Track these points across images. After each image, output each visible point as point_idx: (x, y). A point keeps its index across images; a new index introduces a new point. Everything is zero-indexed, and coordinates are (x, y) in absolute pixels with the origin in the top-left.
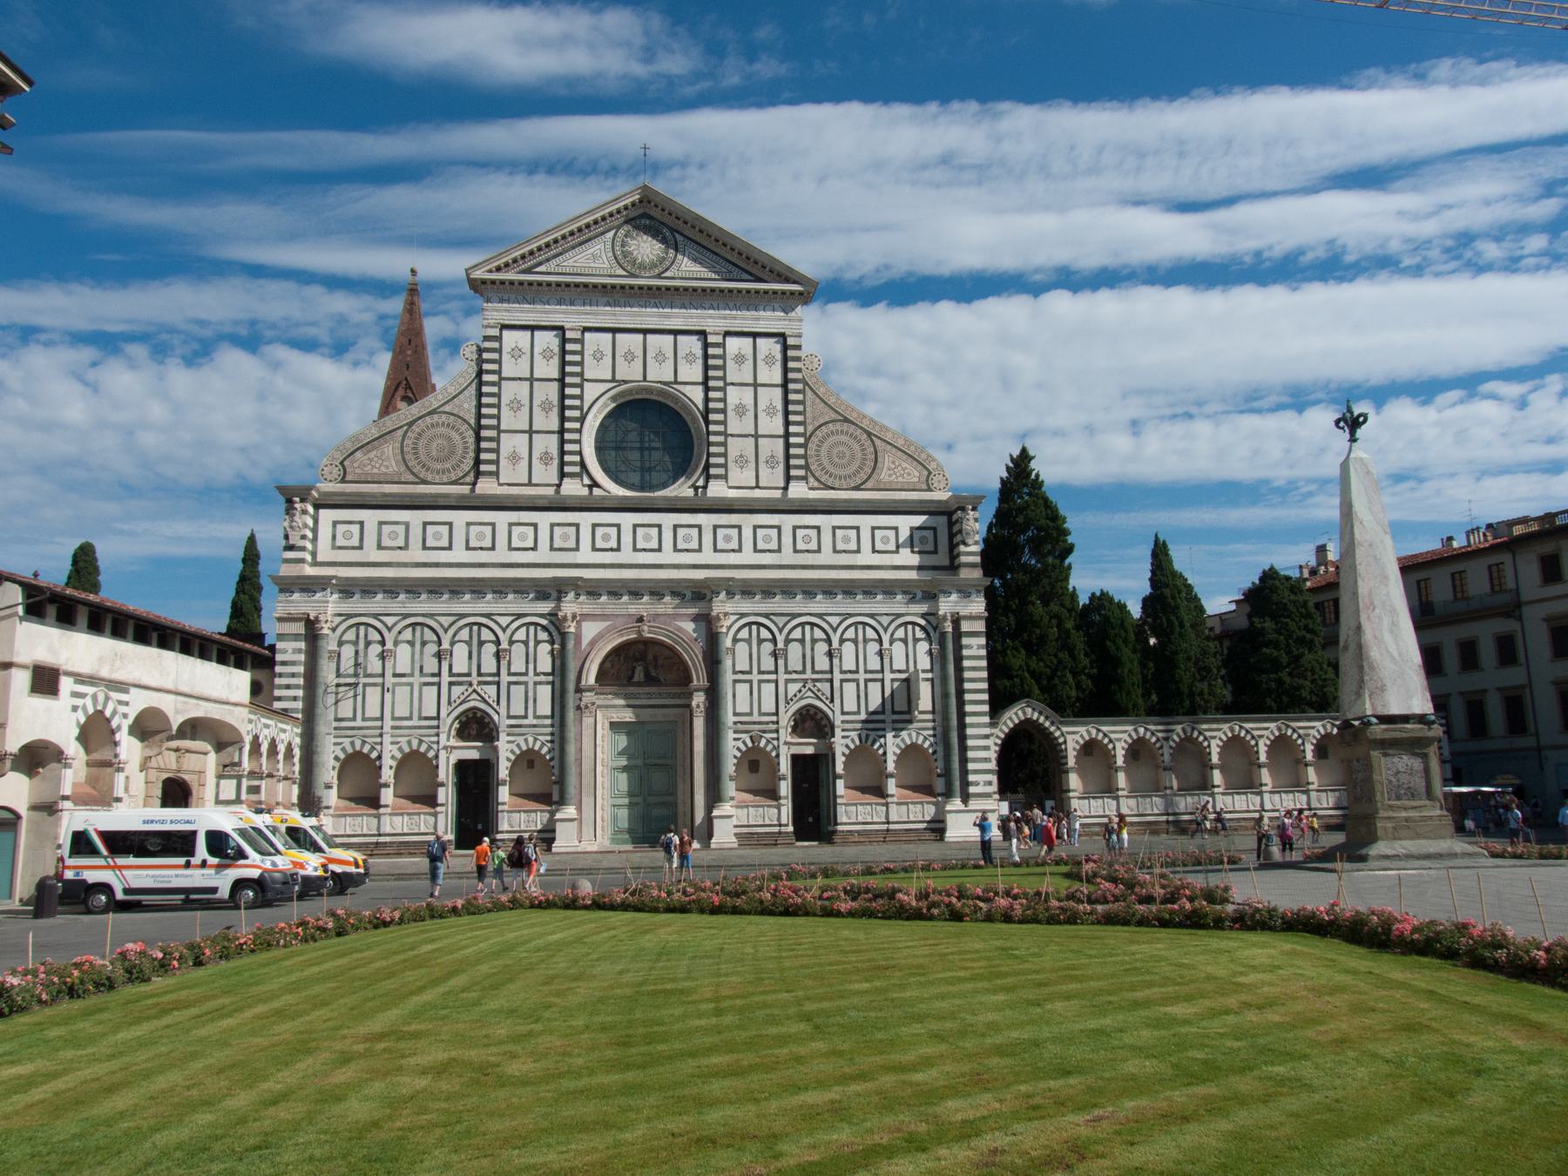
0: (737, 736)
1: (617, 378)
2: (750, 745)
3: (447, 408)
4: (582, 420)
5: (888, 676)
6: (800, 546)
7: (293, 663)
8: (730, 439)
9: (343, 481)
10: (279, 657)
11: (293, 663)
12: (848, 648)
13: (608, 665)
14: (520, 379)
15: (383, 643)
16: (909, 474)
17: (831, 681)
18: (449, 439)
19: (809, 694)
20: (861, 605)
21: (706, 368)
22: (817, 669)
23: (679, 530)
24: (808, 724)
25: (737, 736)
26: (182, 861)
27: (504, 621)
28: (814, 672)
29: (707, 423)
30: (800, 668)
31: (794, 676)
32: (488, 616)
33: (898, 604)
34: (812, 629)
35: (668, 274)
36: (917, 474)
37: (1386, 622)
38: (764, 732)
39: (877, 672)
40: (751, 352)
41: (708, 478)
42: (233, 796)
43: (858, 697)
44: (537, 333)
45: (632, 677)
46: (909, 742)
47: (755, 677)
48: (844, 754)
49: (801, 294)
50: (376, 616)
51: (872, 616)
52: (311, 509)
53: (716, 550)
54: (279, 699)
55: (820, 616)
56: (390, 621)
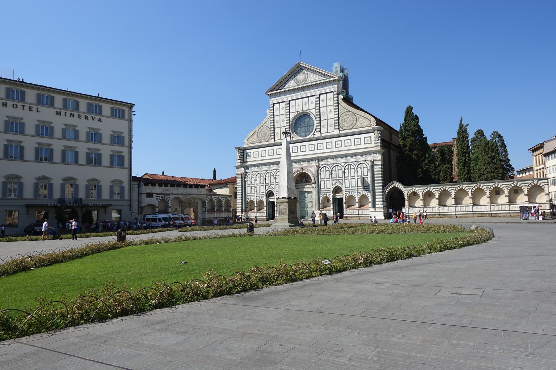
0: (321, 194)
1: (297, 111)
2: (324, 196)
3: (265, 125)
4: (290, 123)
5: (356, 177)
6: (337, 146)
7: (239, 183)
8: (321, 121)
9: (248, 144)
10: (237, 182)
11: (239, 183)
12: (347, 171)
13: (298, 179)
14: (277, 115)
15: (254, 178)
16: (365, 123)
17: (342, 179)
18: (265, 132)
19: (337, 183)
20: (349, 159)
21: (316, 104)
22: (339, 177)
23: (310, 146)
24: (339, 190)
25: (321, 194)
26: (156, 222)
27: (274, 171)
28: (339, 178)
29: (316, 118)
30: (335, 177)
31: (334, 179)
32: (271, 170)
33: (359, 158)
34: (338, 167)
35: (306, 83)
36: (367, 122)
37: (283, 177)
38: (327, 193)
39: (354, 176)
40: (326, 98)
41: (317, 132)
42: (205, 211)
43: (349, 183)
44: (280, 104)
45: (303, 181)
46: (362, 194)
47: (325, 180)
48: (346, 197)
49: (336, 80)
50: (252, 172)
51: (352, 162)
52: (242, 151)
53: (318, 150)
54: (238, 190)
55: (339, 163)
56: (255, 173)
